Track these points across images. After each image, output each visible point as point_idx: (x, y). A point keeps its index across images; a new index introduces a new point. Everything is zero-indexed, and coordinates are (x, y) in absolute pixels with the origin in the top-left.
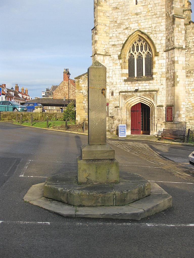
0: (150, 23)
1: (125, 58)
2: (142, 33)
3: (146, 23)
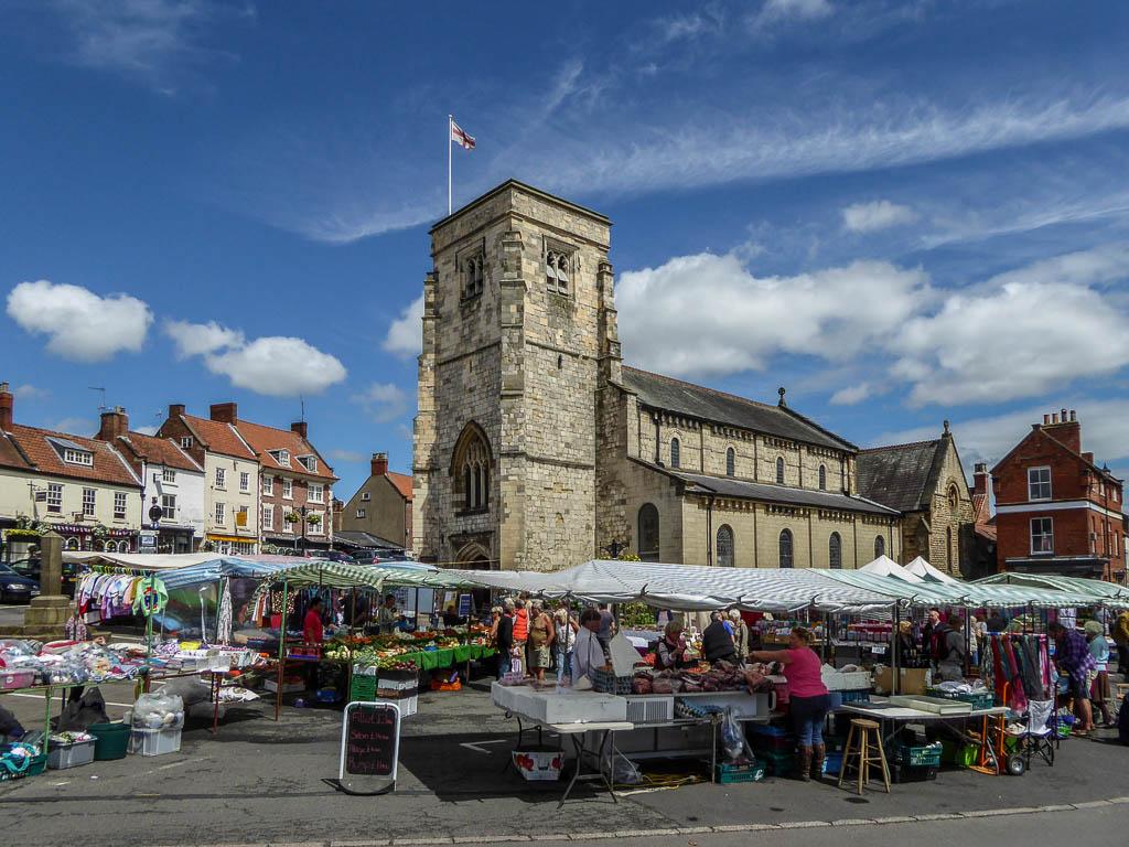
1: (458, 473)
2: (477, 425)
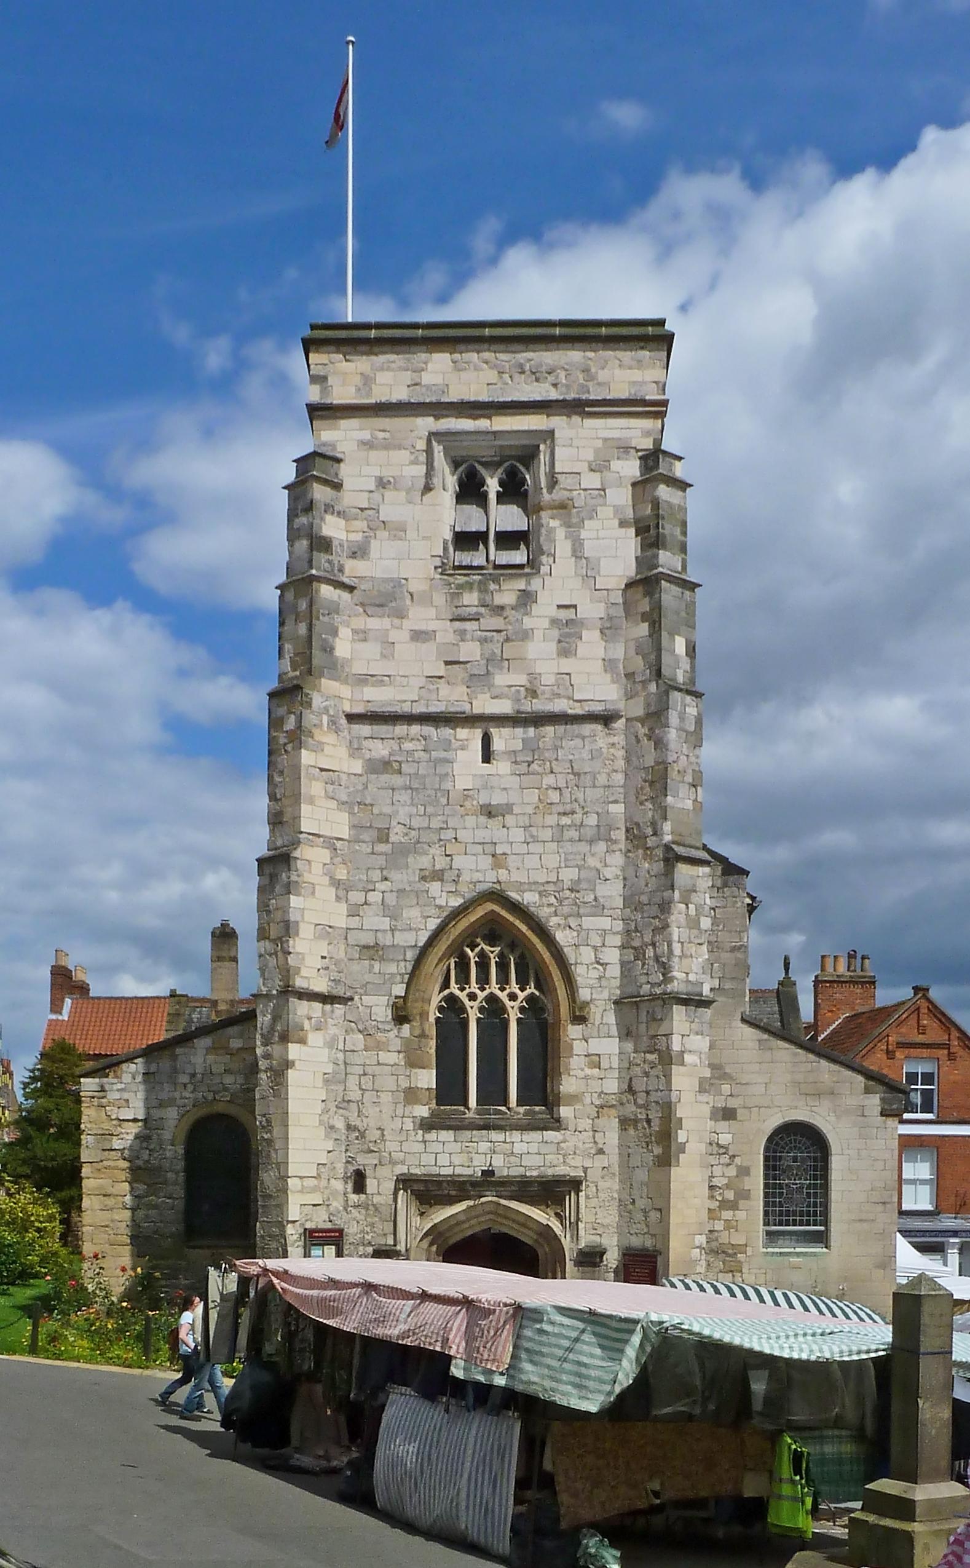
0: (552, 861)
1: (424, 1015)
2: (516, 908)
3: (532, 862)
